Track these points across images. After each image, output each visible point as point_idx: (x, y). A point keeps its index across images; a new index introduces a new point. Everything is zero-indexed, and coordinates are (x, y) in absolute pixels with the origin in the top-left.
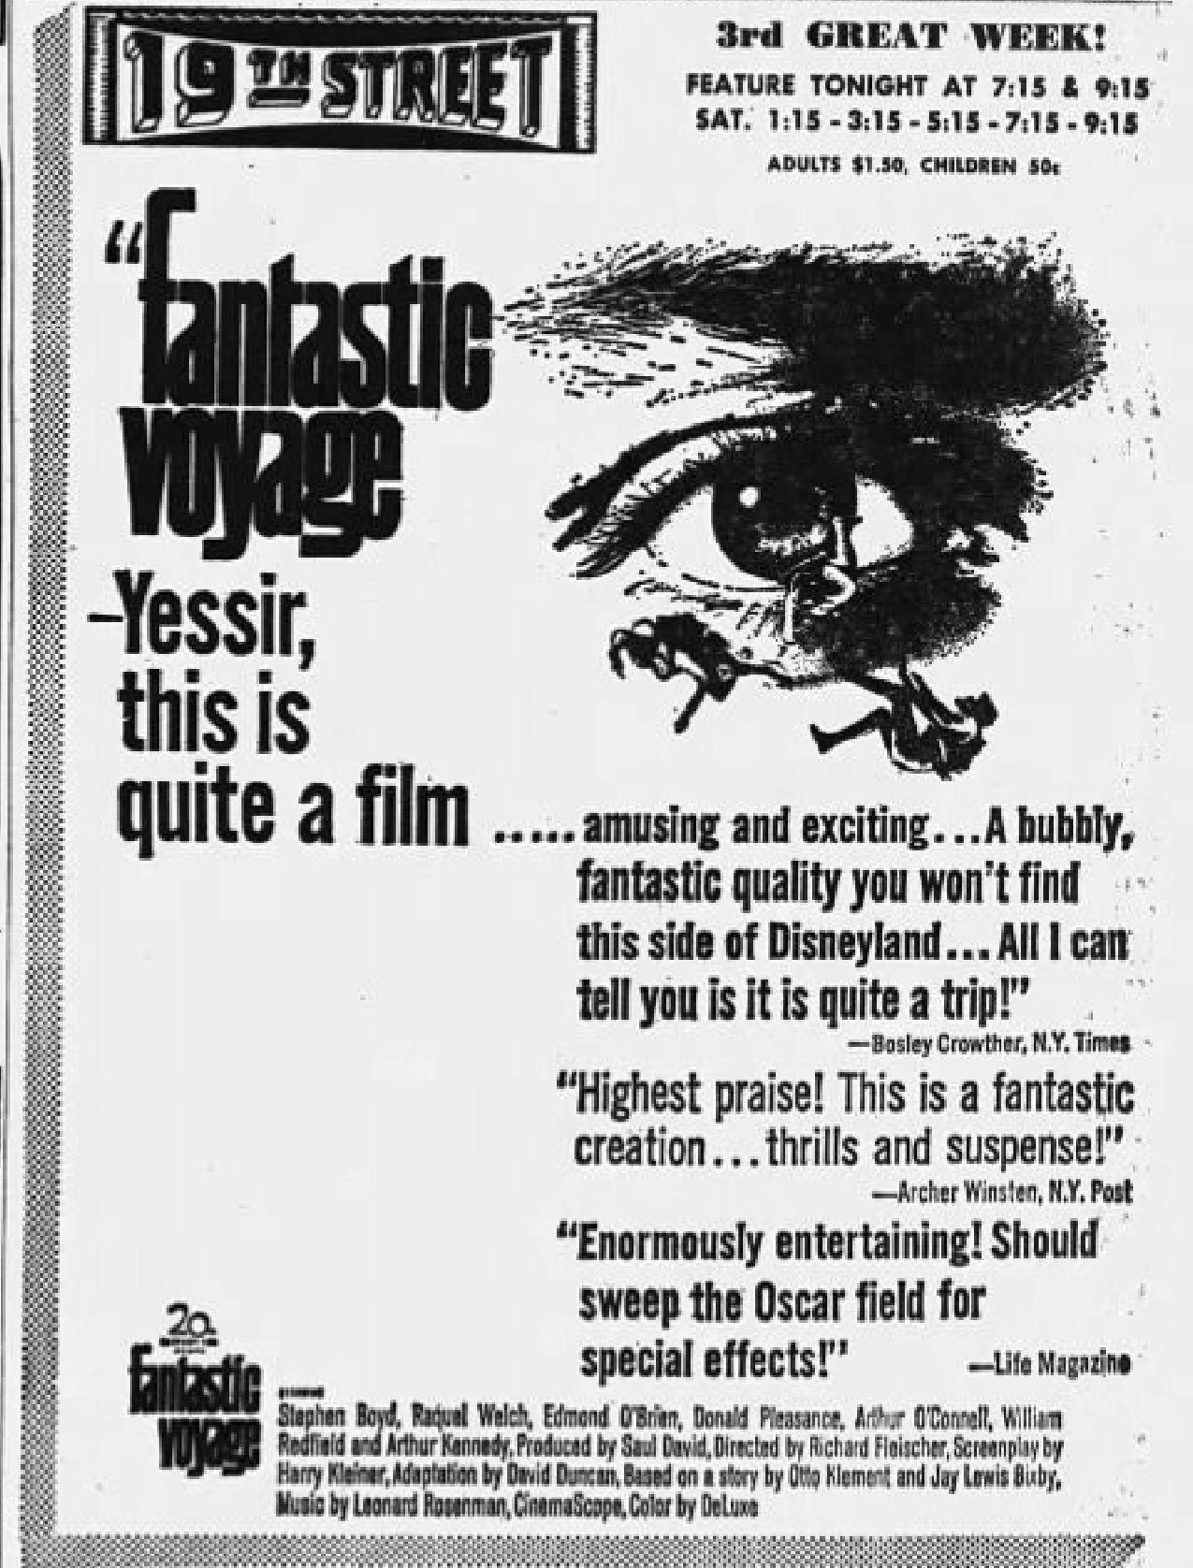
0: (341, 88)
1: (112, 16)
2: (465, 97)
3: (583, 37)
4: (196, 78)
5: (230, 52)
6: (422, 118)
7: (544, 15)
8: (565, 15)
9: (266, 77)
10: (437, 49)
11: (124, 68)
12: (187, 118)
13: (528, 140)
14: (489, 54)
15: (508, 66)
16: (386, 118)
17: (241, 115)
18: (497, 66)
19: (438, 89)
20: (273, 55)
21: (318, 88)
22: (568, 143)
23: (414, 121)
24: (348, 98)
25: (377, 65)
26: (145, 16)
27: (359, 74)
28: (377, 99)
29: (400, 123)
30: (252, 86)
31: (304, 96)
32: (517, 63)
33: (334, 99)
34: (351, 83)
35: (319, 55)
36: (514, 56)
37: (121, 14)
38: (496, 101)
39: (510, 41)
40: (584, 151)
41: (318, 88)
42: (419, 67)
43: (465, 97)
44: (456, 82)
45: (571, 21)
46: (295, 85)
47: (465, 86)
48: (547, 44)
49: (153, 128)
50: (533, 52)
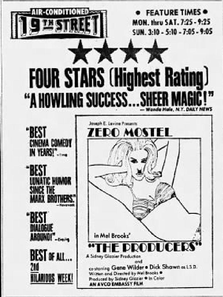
0: (59, 26)
3: (104, 15)
4: (33, 25)
6: (75, 32)
8: (100, 11)
9: (45, 24)
10: (77, 18)
11: (19, 23)
14: (87, 18)
15: (91, 21)
16: (68, 32)
17: (41, 32)
19: (78, 26)
22: (102, 36)
23: (73, 33)
24: (60, 29)
25: (66, 21)
26: (23, 13)
27: (62, 23)
28: (66, 28)
30: (43, 27)
31: (52, 28)
33: (58, 29)
35: (55, 20)
36: (92, 19)
37: (18, 13)
38: (89, 28)
39: (91, 16)
41: (55, 26)
42: (74, 22)
43: (84, 27)
44: (81, 24)
46: (51, 26)
47: (82, 25)
48: (97, 16)
50: (95, 18)
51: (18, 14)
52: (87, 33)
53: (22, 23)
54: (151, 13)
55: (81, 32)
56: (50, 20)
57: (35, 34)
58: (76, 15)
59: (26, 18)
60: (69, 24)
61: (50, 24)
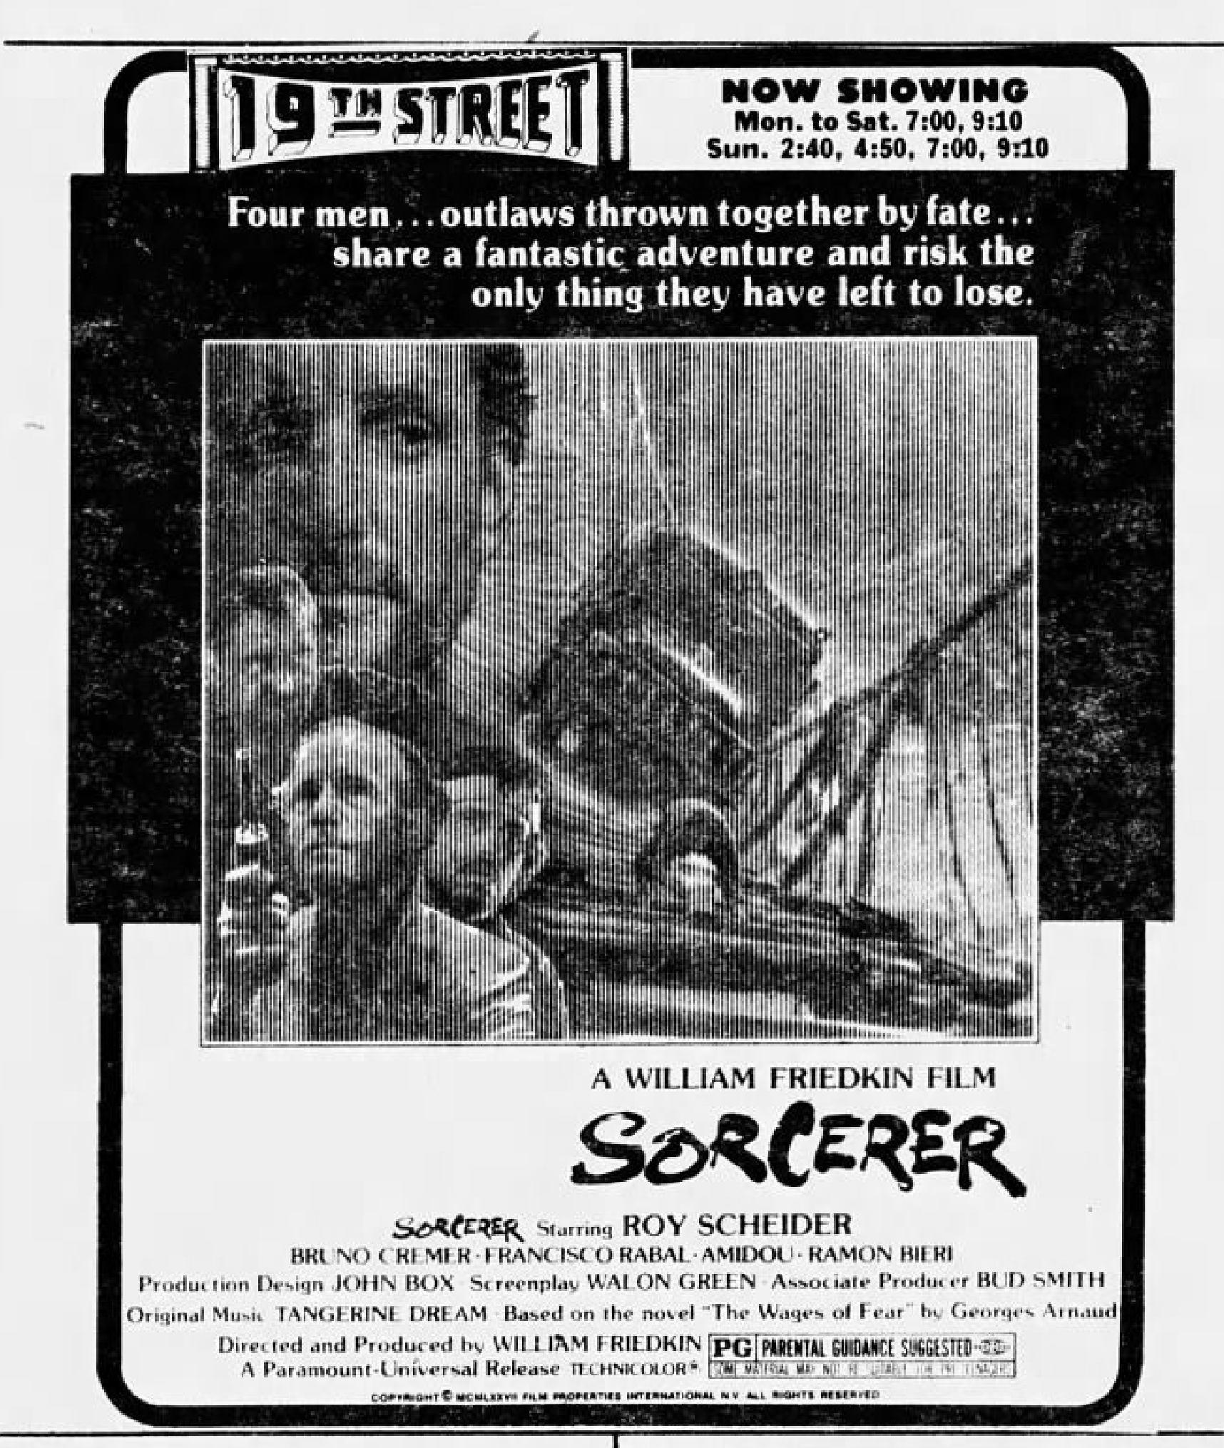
0: (410, 120)
4: (283, 112)
5: (310, 91)
6: (482, 142)
9: (343, 109)
10: (493, 82)
14: (535, 85)
15: (554, 96)
19: (495, 117)
24: (414, 128)
25: (440, 97)
27: (427, 107)
28: (442, 127)
31: (375, 126)
33: (404, 129)
34: (417, 113)
35: (390, 92)
36: (559, 85)
38: (543, 126)
39: (555, 74)
41: (391, 116)
43: (519, 122)
44: (509, 109)
46: (368, 118)
47: (516, 113)
48: (585, 75)
50: (574, 82)
51: (221, 64)
56: (363, 93)
60: (453, 106)
61: (364, 111)
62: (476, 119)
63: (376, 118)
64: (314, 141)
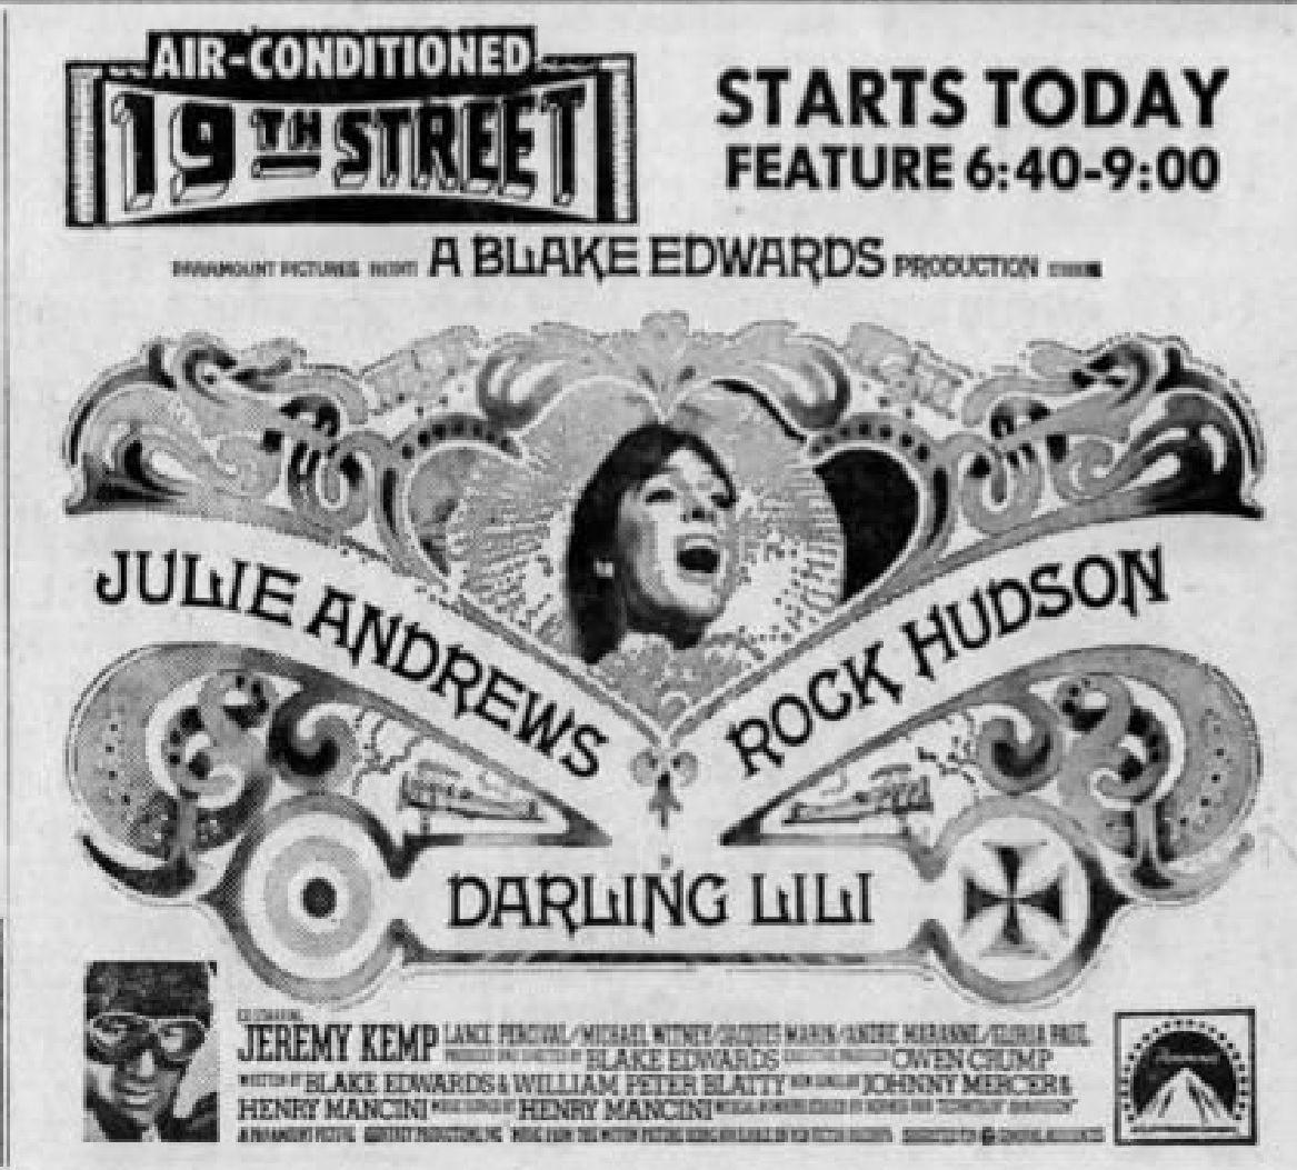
0: (355, 154)
1: (97, 72)
2: (490, 160)
3: (619, 85)
4: (192, 144)
6: (442, 186)
7: (576, 59)
8: (600, 58)
9: (272, 139)
10: (457, 102)
11: (112, 134)
12: (183, 192)
13: (559, 209)
16: (402, 188)
17: (244, 188)
18: (525, 122)
19: (459, 149)
20: (278, 116)
21: (331, 151)
22: (606, 213)
23: (434, 191)
24: (361, 165)
25: (392, 121)
27: (373, 134)
28: (394, 166)
29: (418, 192)
31: (314, 162)
32: (547, 117)
33: (348, 167)
34: (362, 145)
35: (330, 114)
36: (543, 110)
38: (524, 164)
39: (539, 91)
40: (623, 222)
41: (331, 151)
42: (437, 125)
43: (490, 160)
44: (480, 141)
45: (605, 65)
46: (304, 151)
48: (579, 93)
49: (149, 205)
51: (107, 77)
52: (514, 194)
53: (130, 128)
54: (763, 167)
55: (478, 189)
57: (204, 196)
58: (450, 83)
59: (149, 102)
62: (435, 154)
63: (314, 152)
64: (234, 182)
